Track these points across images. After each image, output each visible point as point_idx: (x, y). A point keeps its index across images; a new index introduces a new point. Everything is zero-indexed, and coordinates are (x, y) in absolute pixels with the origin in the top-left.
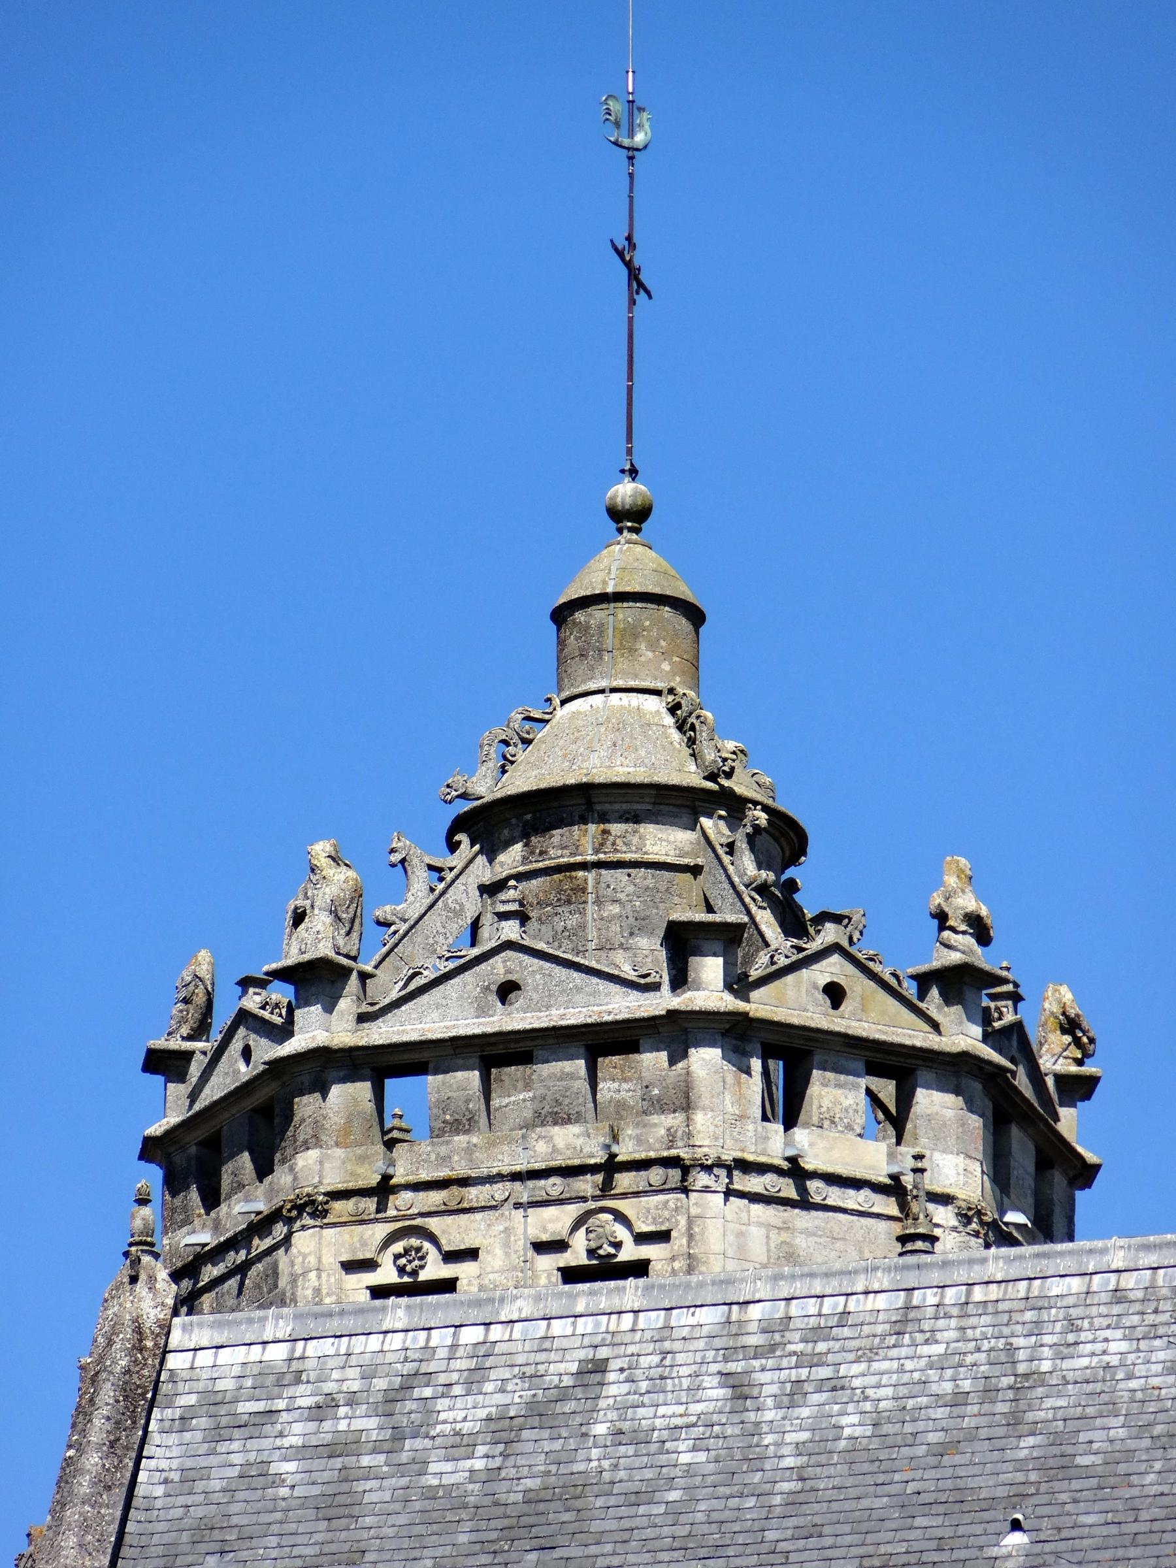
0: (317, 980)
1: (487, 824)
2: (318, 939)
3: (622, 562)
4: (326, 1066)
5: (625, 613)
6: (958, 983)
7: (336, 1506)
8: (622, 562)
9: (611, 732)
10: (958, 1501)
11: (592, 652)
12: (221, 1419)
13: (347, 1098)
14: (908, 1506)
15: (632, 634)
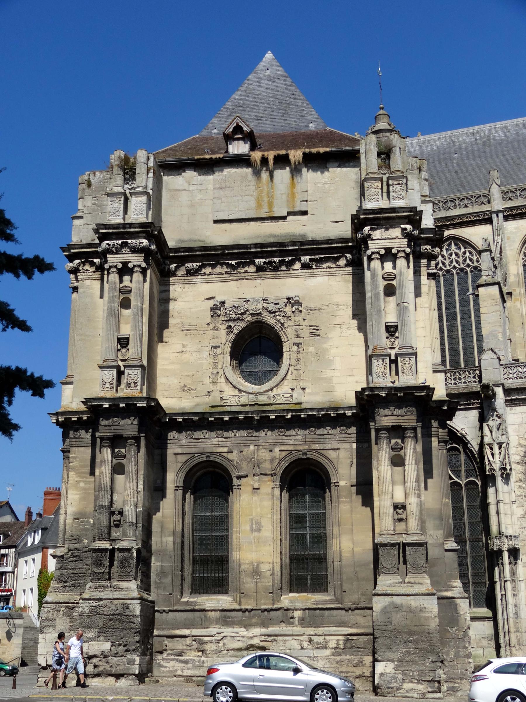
3: (382, 112)
5: (383, 115)
10: (448, 153)
11: (380, 119)
14: (443, 154)
15: (383, 118)
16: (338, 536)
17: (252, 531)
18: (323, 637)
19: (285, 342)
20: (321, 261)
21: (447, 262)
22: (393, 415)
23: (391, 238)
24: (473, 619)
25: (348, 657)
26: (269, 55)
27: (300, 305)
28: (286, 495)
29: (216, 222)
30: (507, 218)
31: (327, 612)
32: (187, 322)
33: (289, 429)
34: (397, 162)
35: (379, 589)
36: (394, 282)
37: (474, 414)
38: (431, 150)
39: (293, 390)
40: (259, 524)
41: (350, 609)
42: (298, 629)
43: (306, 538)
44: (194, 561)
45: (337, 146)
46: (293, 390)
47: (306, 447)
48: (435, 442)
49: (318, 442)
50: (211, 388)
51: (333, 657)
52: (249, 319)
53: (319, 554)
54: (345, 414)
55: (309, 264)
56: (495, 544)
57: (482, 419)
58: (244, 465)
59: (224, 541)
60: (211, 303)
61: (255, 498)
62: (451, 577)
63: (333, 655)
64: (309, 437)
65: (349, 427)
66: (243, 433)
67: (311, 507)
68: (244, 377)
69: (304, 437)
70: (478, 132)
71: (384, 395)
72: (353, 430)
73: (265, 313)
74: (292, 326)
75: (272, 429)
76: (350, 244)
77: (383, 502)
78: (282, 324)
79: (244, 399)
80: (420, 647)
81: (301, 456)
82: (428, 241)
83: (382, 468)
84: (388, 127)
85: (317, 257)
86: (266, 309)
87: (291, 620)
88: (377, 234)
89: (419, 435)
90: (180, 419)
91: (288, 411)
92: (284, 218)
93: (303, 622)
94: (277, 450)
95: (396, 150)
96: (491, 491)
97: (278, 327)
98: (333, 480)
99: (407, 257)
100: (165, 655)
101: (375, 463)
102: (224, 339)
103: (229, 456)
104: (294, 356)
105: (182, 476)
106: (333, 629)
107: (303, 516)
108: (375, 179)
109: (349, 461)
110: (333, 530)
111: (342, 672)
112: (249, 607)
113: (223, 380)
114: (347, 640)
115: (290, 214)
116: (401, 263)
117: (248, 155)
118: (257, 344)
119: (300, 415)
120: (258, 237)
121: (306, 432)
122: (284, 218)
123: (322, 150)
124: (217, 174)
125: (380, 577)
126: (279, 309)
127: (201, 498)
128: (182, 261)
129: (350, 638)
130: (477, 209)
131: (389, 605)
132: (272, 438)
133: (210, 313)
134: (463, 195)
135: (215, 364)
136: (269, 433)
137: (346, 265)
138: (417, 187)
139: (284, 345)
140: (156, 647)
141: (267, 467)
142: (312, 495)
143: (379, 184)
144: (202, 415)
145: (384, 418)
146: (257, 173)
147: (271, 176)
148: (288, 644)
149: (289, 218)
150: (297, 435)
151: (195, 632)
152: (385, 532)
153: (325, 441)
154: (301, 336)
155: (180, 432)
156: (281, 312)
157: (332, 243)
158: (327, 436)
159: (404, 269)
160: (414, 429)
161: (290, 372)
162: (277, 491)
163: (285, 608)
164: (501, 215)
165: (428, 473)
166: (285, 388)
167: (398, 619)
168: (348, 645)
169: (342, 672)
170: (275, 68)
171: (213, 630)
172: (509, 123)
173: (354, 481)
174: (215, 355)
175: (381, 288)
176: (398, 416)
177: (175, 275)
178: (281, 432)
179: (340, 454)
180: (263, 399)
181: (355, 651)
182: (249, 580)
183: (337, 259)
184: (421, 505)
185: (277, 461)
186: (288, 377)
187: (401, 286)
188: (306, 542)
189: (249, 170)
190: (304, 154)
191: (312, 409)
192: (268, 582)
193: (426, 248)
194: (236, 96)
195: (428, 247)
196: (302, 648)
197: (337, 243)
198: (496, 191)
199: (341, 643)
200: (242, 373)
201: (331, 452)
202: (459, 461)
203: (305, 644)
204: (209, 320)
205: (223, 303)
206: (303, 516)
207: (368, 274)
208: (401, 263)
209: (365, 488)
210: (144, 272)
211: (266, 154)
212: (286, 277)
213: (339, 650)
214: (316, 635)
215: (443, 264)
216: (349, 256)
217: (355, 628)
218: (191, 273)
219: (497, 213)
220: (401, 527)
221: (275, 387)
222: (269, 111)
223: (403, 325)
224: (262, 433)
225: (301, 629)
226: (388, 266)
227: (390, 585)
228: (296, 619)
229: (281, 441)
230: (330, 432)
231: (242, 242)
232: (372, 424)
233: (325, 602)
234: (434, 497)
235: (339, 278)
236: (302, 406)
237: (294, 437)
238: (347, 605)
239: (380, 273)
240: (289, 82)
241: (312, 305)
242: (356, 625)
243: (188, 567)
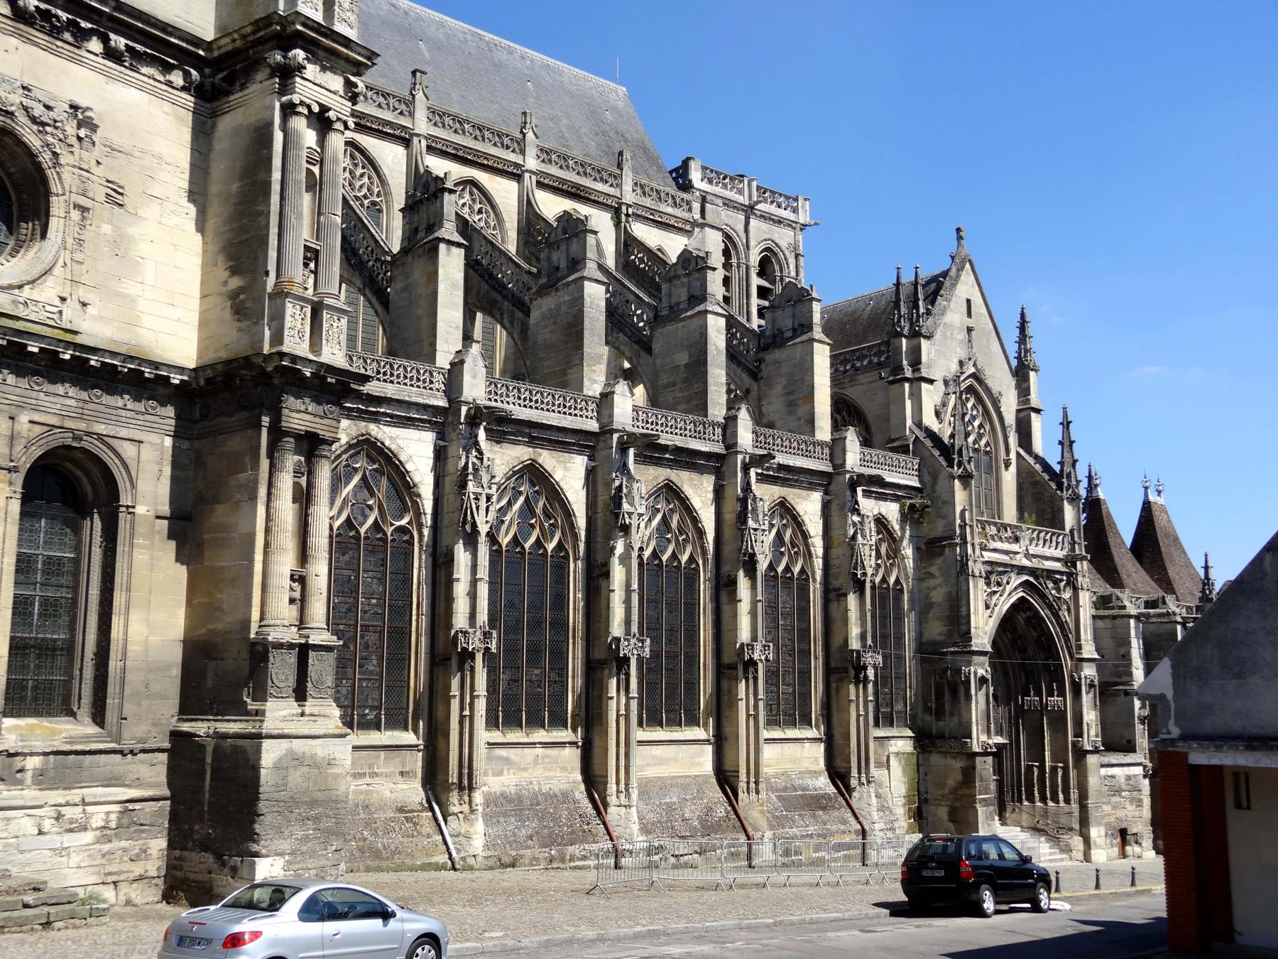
16: (123, 611)
18: (80, 809)
19: (57, 195)
22: (306, 412)
25: (124, 844)
27: (94, 128)
31: (88, 758)
33: (53, 381)
39: (63, 299)
41: (132, 752)
42: (30, 795)
43: (33, 604)
46: (63, 299)
47: (82, 426)
49: (106, 420)
51: (97, 846)
53: (55, 640)
54: (169, 377)
55: (122, 54)
63: (98, 841)
64: (91, 406)
69: (81, 405)
71: (308, 374)
72: (170, 411)
73: (22, 117)
74: (74, 166)
75: (20, 373)
76: (201, 52)
78: (55, 154)
80: (322, 826)
81: (69, 442)
85: (139, 47)
86: (26, 109)
87: (18, 775)
91: (69, 345)
93: (43, 779)
94: (24, 418)
97: (45, 158)
98: (125, 500)
106: (99, 792)
109: (156, 468)
111: (110, 874)
114: (125, 812)
119: (88, 360)
121: (84, 395)
125: (268, 704)
126: (55, 121)
129: (131, 806)
131: (286, 755)
132: (18, 391)
137: (183, 89)
139: (53, 199)
145: (294, 415)
148: (13, 827)
150: (66, 396)
152: (278, 622)
153: (118, 422)
154: (90, 195)
156: (56, 128)
157: (171, 34)
158: (123, 413)
161: (60, 263)
163: (12, 751)
166: (47, 292)
168: (125, 821)
169: (110, 874)
173: (165, 509)
176: (315, 415)
178: (37, 384)
181: (136, 831)
185: (24, 441)
186: (58, 270)
188: (32, 614)
191: (114, 354)
196: (40, 833)
197: (179, 38)
199: (113, 817)
201: (126, 444)
203: (48, 825)
212: (71, 59)
213: (109, 832)
214: (68, 804)
217: (136, 787)
221: (29, 283)
225: (38, 792)
227: (285, 719)
228: (29, 775)
229: (33, 402)
230: (129, 407)
235: (167, 107)
236: (79, 339)
237: (61, 400)
238: (127, 744)
241: (117, 141)
242: (138, 783)
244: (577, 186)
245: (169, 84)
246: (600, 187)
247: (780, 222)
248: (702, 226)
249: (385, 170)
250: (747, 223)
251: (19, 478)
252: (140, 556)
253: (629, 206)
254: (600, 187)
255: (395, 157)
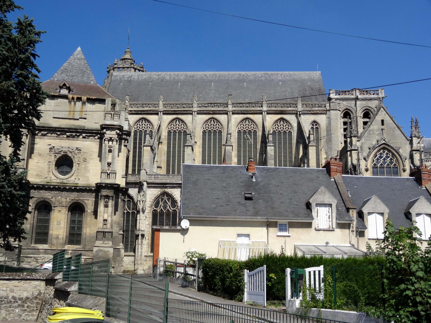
0: (115, 64)
1: (122, 60)
2: (116, 62)
3: (128, 50)
4: (116, 68)
6: (142, 67)
7: (121, 80)
8: (128, 50)
9: (127, 56)
10: (148, 82)
12: (115, 76)
13: (116, 69)
17: (57, 224)
20: (89, 136)
21: (141, 127)
23: (112, 134)
24: (125, 256)
26: (79, 49)
27: (81, 150)
28: (70, 213)
29: (54, 118)
30: (164, 114)
32: (40, 152)
34: (117, 108)
35: (96, 245)
36: (112, 149)
37: (137, 190)
38: (142, 79)
40: (60, 222)
44: (36, 233)
45: (99, 96)
47: (78, 198)
48: (120, 200)
50: (47, 176)
52: (63, 153)
56: (137, 233)
57: (139, 192)
58: (56, 203)
59: (47, 228)
60: (50, 147)
61: (59, 214)
62: (120, 242)
65: (93, 193)
66: (57, 192)
67: (78, 218)
68: (59, 172)
70: (160, 75)
72: (94, 194)
73: (68, 152)
75: (67, 192)
77: (100, 219)
79: (58, 181)
82: (125, 134)
83: (101, 208)
84: (130, 58)
85: (88, 135)
88: (108, 132)
89: (114, 198)
90: (35, 186)
91: (73, 186)
92: (78, 119)
94: (68, 199)
95: (117, 105)
96: (138, 215)
97: (72, 158)
99: (117, 141)
100: (24, 263)
101: (99, 206)
102: (53, 160)
103: (52, 199)
104: (77, 168)
105: (34, 205)
107: (75, 220)
108: (109, 114)
110: (84, 226)
112: (54, 249)
113: (52, 173)
114: (85, 260)
115: (80, 118)
116: (115, 143)
117: (67, 95)
118: (64, 163)
120: (68, 125)
121: (78, 194)
122: (78, 119)
123: (93, 98)
124: (55, 100)
127: (40, 212)
128: (40, 130)
130: (153, 109)
133: (49, 150)
134: (149, 103)
135: (49, 168)
136: (66, 193)
138: (124, 115)
140: (21, 260)
141: (64, 204)
142: (79, 214)
143: (110, 115)
144: (44, 186)
146: (70, 102)
147: (75, 104)
149: (80, 120)
151: (35, 256)
153: (84, 197)
155: (35, 190)
159: (115, 145)
160: (113, 197)
162: (67, 212)
164: (162, 113)
165: (116, 210)
166: (73, 178)
167: (101, 254)
170: (81, 55)
171: (41, 256)
172: (172, 73)
173: (93, 211)
174: (50, 165)
175: (107, 150)
177: (37, 135)
179: (89, 201)
180: (65, 181)
182: (55, 240)
183: (95, 136)
184: (112, 220)
187: (114, 150)
189: (67, 101)
190: (87, 98)
191: (81, 187)
192: (61, 241)
193: (124, 136)
194: (65, 65)
195: (125, 136)
198: (161, 103)
200: (58, 171)
202: (130, 205)
204: (48, 152)
205: (54, 147)
206: (75, 220)
207: (103, 145)
208: (115, 143)
209: (95, 213)
210: (27, 136)
211: (74, 96)
215: (139, 127)
216: (99, 136)
218: (43, 135)
219: (161, 112)
220: (105, 226)
222: (77, 73)
223: (113, 163)
224: (64, 193)
226: (110, 143)
231: (62, 127)
232: (99, 194)
233: (79, 248)
234: (118, 217)
235: (95, 143)
236: (78, 185)
238: (86, 249)
239: (107, 145)
240: (85, 62)
241: (85, 151)
242: (88, 256)
243: (34, 235)
244: (282, 111)
245: (95, 139)
246: (290, 109)
247: (371, 100)
248: (329, 110)
249: (222, 122)
250: (356, 103)
251: (68, 208)
252: (89, 219)
253: (300, 112)
254: (290, 109)
255: (224, 118)
